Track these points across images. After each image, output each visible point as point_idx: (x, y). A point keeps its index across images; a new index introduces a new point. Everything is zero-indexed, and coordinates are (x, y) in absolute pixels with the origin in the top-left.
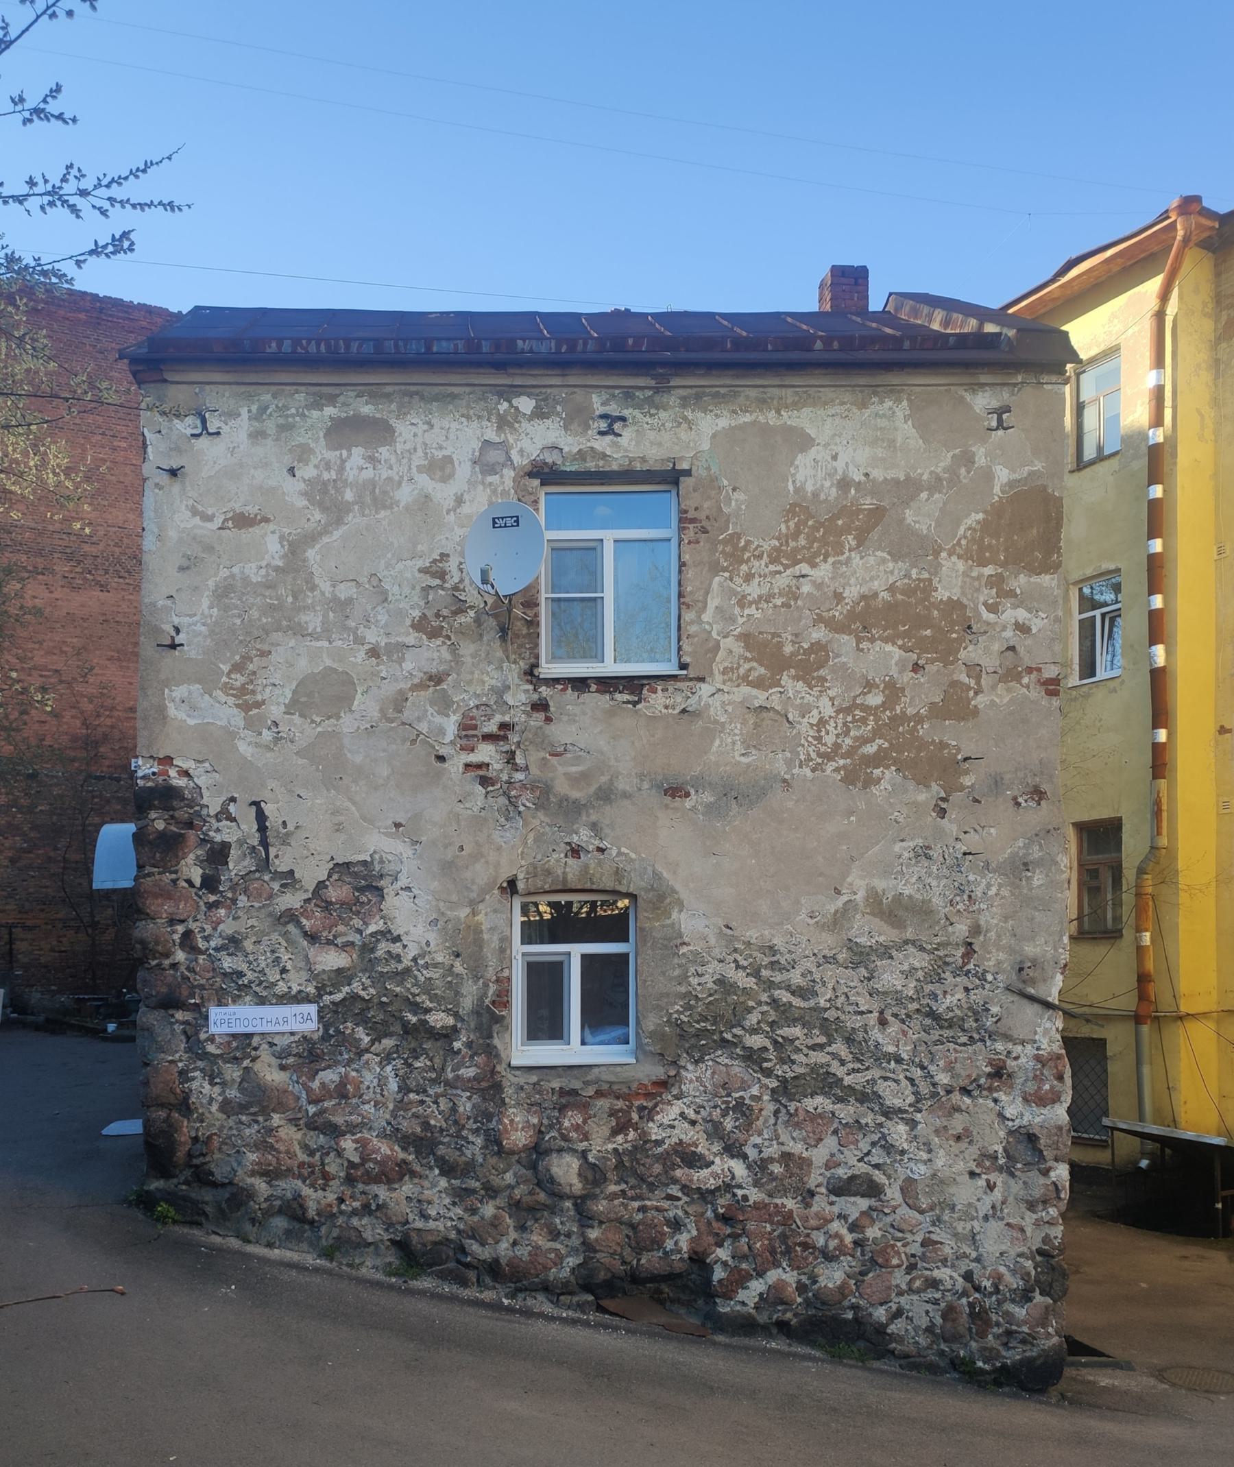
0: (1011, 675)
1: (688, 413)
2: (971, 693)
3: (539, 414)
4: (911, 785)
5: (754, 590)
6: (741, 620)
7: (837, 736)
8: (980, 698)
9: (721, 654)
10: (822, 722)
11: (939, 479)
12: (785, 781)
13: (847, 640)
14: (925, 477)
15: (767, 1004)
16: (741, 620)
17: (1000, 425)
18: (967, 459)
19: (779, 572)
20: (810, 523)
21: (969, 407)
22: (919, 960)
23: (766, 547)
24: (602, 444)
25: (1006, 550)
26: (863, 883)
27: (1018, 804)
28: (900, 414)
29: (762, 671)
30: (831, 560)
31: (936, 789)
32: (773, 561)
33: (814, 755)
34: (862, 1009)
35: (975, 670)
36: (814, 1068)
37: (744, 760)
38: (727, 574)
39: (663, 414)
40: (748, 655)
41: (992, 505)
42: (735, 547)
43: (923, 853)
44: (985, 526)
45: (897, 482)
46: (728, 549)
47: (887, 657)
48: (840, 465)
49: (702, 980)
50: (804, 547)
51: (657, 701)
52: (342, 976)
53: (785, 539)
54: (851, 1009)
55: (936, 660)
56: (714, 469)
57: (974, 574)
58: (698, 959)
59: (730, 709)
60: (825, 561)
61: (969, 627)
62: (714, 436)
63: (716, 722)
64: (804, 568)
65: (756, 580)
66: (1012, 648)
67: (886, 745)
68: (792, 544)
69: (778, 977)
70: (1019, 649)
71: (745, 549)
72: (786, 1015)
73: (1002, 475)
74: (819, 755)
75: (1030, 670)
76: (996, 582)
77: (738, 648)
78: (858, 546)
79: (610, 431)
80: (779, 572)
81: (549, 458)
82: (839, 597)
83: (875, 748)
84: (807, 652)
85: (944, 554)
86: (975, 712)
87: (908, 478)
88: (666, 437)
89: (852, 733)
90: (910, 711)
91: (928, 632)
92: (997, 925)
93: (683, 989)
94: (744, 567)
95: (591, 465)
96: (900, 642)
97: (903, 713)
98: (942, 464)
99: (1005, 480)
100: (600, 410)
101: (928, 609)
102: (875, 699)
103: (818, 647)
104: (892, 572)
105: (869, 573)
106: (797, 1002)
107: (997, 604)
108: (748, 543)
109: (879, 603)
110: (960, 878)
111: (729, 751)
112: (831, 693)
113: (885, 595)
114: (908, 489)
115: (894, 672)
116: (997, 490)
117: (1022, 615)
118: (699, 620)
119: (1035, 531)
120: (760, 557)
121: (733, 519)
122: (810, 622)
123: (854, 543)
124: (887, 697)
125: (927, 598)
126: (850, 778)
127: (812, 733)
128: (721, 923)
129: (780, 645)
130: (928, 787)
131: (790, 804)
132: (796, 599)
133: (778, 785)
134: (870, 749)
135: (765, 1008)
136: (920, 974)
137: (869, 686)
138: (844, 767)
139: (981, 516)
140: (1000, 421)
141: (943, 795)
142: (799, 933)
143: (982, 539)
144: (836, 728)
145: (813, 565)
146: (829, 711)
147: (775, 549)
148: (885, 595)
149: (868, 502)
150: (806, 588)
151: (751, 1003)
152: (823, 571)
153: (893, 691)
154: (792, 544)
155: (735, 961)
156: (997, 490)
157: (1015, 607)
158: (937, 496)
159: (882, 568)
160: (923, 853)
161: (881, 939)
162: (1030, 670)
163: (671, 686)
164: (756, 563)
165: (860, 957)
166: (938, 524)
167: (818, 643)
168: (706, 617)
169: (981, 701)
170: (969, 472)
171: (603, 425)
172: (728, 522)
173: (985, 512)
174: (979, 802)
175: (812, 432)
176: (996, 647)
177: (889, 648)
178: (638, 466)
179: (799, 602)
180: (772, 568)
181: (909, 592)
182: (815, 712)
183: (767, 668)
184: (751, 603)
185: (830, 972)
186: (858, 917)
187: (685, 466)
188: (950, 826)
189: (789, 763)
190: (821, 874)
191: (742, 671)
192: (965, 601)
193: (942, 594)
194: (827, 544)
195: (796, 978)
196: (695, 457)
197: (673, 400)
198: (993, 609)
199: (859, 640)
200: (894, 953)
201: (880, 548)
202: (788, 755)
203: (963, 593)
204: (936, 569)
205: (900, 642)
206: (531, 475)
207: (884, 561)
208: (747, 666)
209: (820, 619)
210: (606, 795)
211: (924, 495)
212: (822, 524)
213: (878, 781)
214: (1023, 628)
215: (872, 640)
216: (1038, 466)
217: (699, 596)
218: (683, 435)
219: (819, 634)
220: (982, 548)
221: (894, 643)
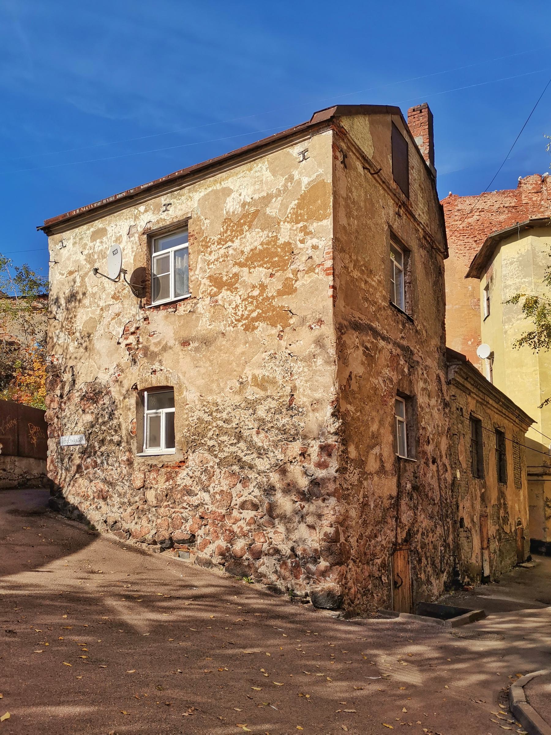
0: (311, 270)
1: (191, 195)
2: (294, 282)
3: (146, 211)
4: (269, 327)
5: (212, 258)
6: (208, 271)
7: (243, 311)
8: (297, 283)
9: (202, 286)
10: (237, 306)
11: (280, 191)
12: (223, 333)
13: (246, 269)
14: (274, 192)
15: (216, 427)
16: (208, 271)
17: (304, 159)
18: (291, 178)
19: (221, 248)
20: (231, 225)
21: (292, 155)
22: (274, 404)
23: (216, 239)
24: (164, 216)
25: (307, 214)
26: (250, 373)
27: (312, 328)
28: (264, 168)
29: (215, 289)
30: (239, 238)
31: (279, 327)
32: (219, 244)
33: (234, 321)
34: (250, 427)
35: (296, 272)
37: (210, 327)
38: (203, 254)
39: (183, 198)
40: (211, 284)
41: (301, 195)
42: (206, 242)
43: (273, 357)
44: (299, 206)
45: (264, 197)
46: (204, 243)
47: (260, 273)
48: (242, 197)
49: (194, 418)
50: (229, 235)
51: (182, 309)
53: (222, 234)
54: (246, 427)
55: (280, 270)
56: (199, 213)
57: (294, 228)
58: (192, 410)
59: (205, 307)
60: (237, 239)
61: (293, 252)
62: (199, 200)
63: (200, 314)
64: (230, 244)
65: (213, 253)
66: (310, 258)
67: (261, 311)
68: (225, 235)
69: (219, 415)
70: (315, 257)
71: (209, 242)
72: (222, 431)
73: (305, 180)
74: (236, 320)
75: (319, 265)
76: (304, 229)
77: (207, 282)
78: (249, 229)
79: (166, 210)
80: (221, 248)
81: (148, 226)
82: (242, 252)
83: (257, 313)
84: (231, 278)
85: (282, 223)
86: (296, 289)
87: (268, 194)
88: (184, 205)
89: (248, 309)
90: (270, 295)
91: (276, 259)
92: (303, 385)
94: (209, 249)
95: (161, 225)
96: (265, 266)
97: (267, 296)
98: (281, 184)
99: (306, 182)
100: (164, 203)
101: (276, 248)
102: (256, 293)
103: (236, 275)
104: (262, 237)
105: (253, 239)
106: (225, 425)
107: (304, 239)
108: (210, 239)
109: (257, 251)
110: (287, 366)
111: (204, 325)
112: (240, 293)
113: (260, 247)
114: (267, 200)
115: (263, 280)
116: (303, 188)
117: (315, 241)
118: (195, 274)
119: (319, 201)
120: (214, 244)
121: (205, 231)
122: (232, 265)
123: (247, 228)
124: (260, 290)
125: (275, 244)
126: (247, 328)
127: (233, 312)
128: (199, 394)
129: (222, 277)
130: (276, 327)
131: (224, 343)
132: (227, 257)
133: (220, 336)
134: (254, 314)
135: (215, 429)
136: (273, 410)
137: (254, 287)
138: (245, 324)
139: (296, 202)
140: (304, 156)
141: (282, 329)
142: (227, 397)
143: (297, 212)
144: (242, 308)
145: (233, 242)
146: (239, 301)
147: (220, 239)
148: (260, 247)
149: (252, 209)
150: (231, 252)
151: (210, 427)
152: (237, 243)
153: (263, 287)
154: (225, 235)
155: (204, 410)
156: (303, 188)
157: (312, 238)
158: (279, 198)
159: (258, 236)
160: (273, 357)
161: (257, 396)
162: (319, 265)
163: (186, 302)
164: (212, 246)
165: (252, 405)
166: (280, 210)
167: (235, 274)
168: (197, 273)
169: (298, 285)
170: (291, 184)
171: (164, 208)
172: (203, 233)
173: (298, 199)
174: (295, 330)
175: (232, 187)
176: (304, 258)
177: (261, 269)
178: (175, 220)
179: (229, 258)
180: (218, 247)
181: (268, 243)
182: (234, 303)
183: (217, 288)
184: (211, 263)
185: (237, 413)
186: (249, 387)
187: (189, 215)
188: (283, 343)
189: (225, 325)
190: (235, 371)
191: (209, 291)
192: (291, 241)
193: (281, 241)
194: (237, 232)
195: (224, 415)
196: (193, 211)
197: (186, 190)
198: (302, 242)
199: (250, 268)
200: (262, 402)
201: (257, 228)
202: (225, 322)
203: (290, 238)
204: (278, 231)
205: (265, 266)
206: (144, 234)
207: (259, 232)
208: (210, 289)
209: (236, 264)
210: (165, 348)
211: (274, 200)
212: (236, 224)
213: (257, 328)
214: (315, 247)
215: (254, 268)
216: (321, 171)
217: (194, 265)
218: (189, 204)
219: (236, 269)
220: (297, 217)
221: (263, 267)
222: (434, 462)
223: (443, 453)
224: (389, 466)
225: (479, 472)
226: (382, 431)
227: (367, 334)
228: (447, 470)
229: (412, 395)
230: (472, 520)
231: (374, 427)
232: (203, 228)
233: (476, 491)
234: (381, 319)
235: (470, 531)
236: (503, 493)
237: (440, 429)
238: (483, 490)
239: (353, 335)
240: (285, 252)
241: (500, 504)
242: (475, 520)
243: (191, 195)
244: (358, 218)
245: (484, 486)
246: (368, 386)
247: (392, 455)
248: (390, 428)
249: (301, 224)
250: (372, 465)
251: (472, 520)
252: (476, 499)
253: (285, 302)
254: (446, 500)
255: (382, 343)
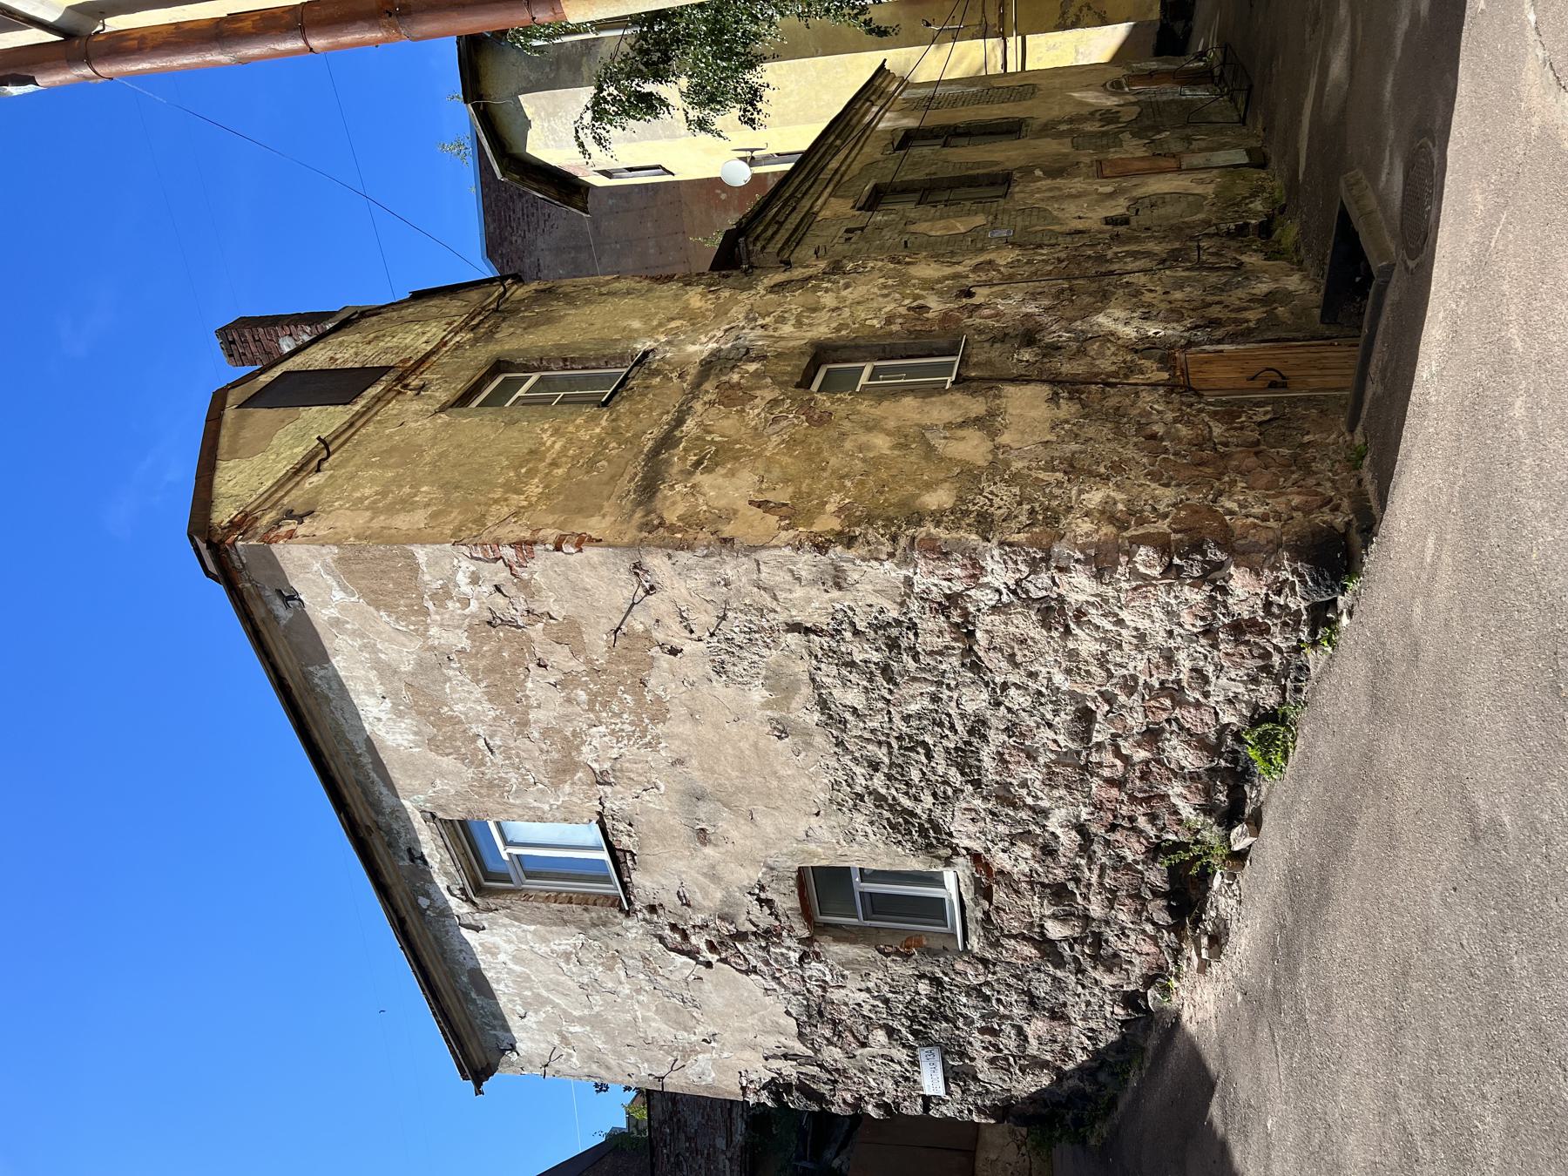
1: (388, 811)
3: (427, 895)
13: (532, 716)
26: (759, 713)
28: (322, 673)
36: (951, 762)
39: (395, 826)
44: (390, 609)
45: (381, 675)
48: (384, 716)
51: (625, 842)
52: (891, 1032)
61: (489, 623)
66: (498, 589)
73: (338, 595)
87: (373, 668)
93: (881, 845)
99: (342, 595)
100: (407, 862)
105: (467, 699)
112: (585, 727)
117: (462, 578)
177: (529, 685)
188: (689, 647)
193: (465, 643)
198: (465, 602)
199: (531, 707)
203: (459, 627)
214: (475, 580)
215: (527, 697)
216: (317, 566)
222: (970, 294)
223: (948, 271)
224: (977, 407)
225: (1001, 181)
226: (891, 424)
227: (668, 462)
228: (990, 262)
229: (811, 351)
230: (1111, 195)
231: (881, 443)
232: (453, 792)
233: (1039, 190)
234: (638, 427)
235: (1136, 200)
236: (1046, 125)
237: (890, 282)
238: (1038, 173)
239: (665, 497)
240: (490, 637)
241: (1071, 131)
242: (1109, 189)
243: (388, 811)
244: (415, 486)
245: (1027, 171)
246: (786, 460)
247: (948, 397)
248: (886, 404)
249: (430, 604)
250: (972, 448)
251: (1111, 195)
252: (1060, 189)
253: (597, 640)
254: (1060, 261)
255: (690, 424)
